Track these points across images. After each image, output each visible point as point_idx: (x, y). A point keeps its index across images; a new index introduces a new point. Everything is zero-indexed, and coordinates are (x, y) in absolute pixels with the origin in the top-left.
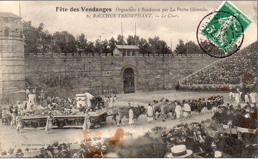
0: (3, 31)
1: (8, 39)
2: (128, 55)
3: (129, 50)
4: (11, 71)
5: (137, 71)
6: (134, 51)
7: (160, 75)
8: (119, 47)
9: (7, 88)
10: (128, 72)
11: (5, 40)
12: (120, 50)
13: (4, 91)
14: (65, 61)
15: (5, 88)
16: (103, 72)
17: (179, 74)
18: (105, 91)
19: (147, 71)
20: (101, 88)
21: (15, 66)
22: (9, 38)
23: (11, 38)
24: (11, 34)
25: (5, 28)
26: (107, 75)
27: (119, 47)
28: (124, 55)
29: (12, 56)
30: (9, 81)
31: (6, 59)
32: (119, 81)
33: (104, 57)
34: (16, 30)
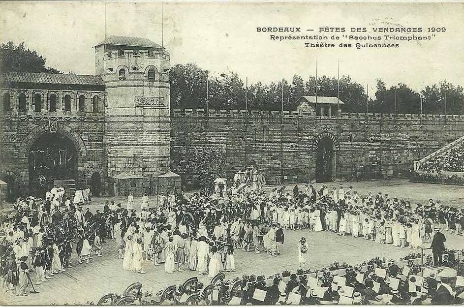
0: (147, 73)
2: (326, 114)
3: (326, 106)
4: (156, 141)
5: (339, 144)
6: (334, 107)
7: (374, 152)
8: (312, 99)
10: (324, 145)
11: (149, 86)
13: (146, 173)
14: (226, 123)
15: (147, 169)
16: (285, 145)
17: (405, 151)
18: (286, 177)
19: (355, 143)
21: (162, 131)
22: (155, 84)
23: (158, 84)
24: (157, 77)
27: (312, 99)
28: (318, 114)
31: (149, 119)
32: (307, 160)
34: (165, 70)
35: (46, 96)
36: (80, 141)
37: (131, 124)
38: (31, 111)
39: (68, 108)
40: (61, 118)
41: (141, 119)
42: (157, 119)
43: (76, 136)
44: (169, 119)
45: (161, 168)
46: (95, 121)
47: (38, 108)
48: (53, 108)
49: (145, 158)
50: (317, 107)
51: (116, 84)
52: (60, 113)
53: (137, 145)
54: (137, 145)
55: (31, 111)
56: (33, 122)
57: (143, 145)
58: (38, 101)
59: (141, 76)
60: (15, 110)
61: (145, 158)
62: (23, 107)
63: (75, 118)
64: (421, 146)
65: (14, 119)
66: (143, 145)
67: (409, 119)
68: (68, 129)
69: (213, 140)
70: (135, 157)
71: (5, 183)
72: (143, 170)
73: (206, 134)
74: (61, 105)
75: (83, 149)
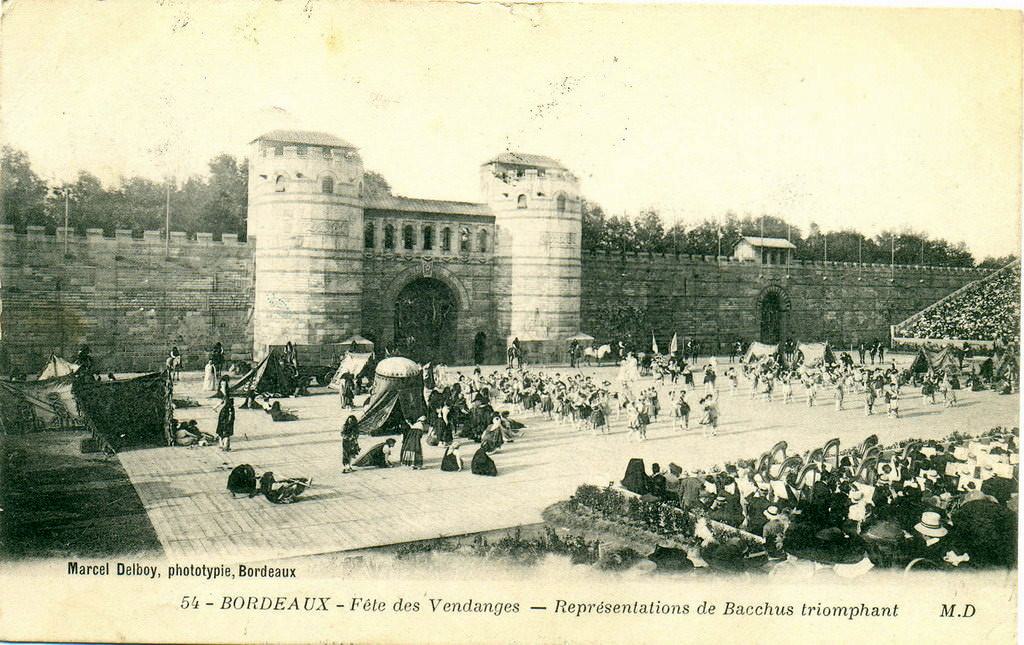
1: (562, 219)
2: (773, 260)
3: (775, 251)
6: (783, 251)
8: (757, 241)
9: (557, 329)
12: (757, 248)
20: (715, 337)
21: (573, 278)
23: (570, 216)
25: (558, 194)
26: (729, 308)
27: (757, 241)
29: (568, 256)
30: (560, 313)
33: (725, 263)
35: (419, 228)
36: (462, 290)
37: (534, 268)
38: (400, 248)
39: (447, 248)
40: (437, 258)
41: (546, 261)
42: (567, 262)
43: (456, 281)
44: (579, 263)
45: (571, 328)
46: (483, 264)
47: (409, 245)
48: (428, 246)
49: (551, 313)
50: (764, 251)
51: (512, 214)
52: (436, 252)
53: (541, 296)
54: (541, 296)
55: (400, 248)
56: (403, 263)
57: (549, 296)
58: (408, 233)
59: (548, 205)
60: (379, 247)
61: (551, 313)
62: (389, 243)
63: (456, 259)
64: (892, 306)
65: (379, 259)
66: (549, 296)
67: (877, 270)
68: (446, 273)
69: (630, 292)
70: (538, 312)
71: (370, 343)
72: (548, 329)
73: (622, 284)
74: (438, 241)
75: (464, 300)
